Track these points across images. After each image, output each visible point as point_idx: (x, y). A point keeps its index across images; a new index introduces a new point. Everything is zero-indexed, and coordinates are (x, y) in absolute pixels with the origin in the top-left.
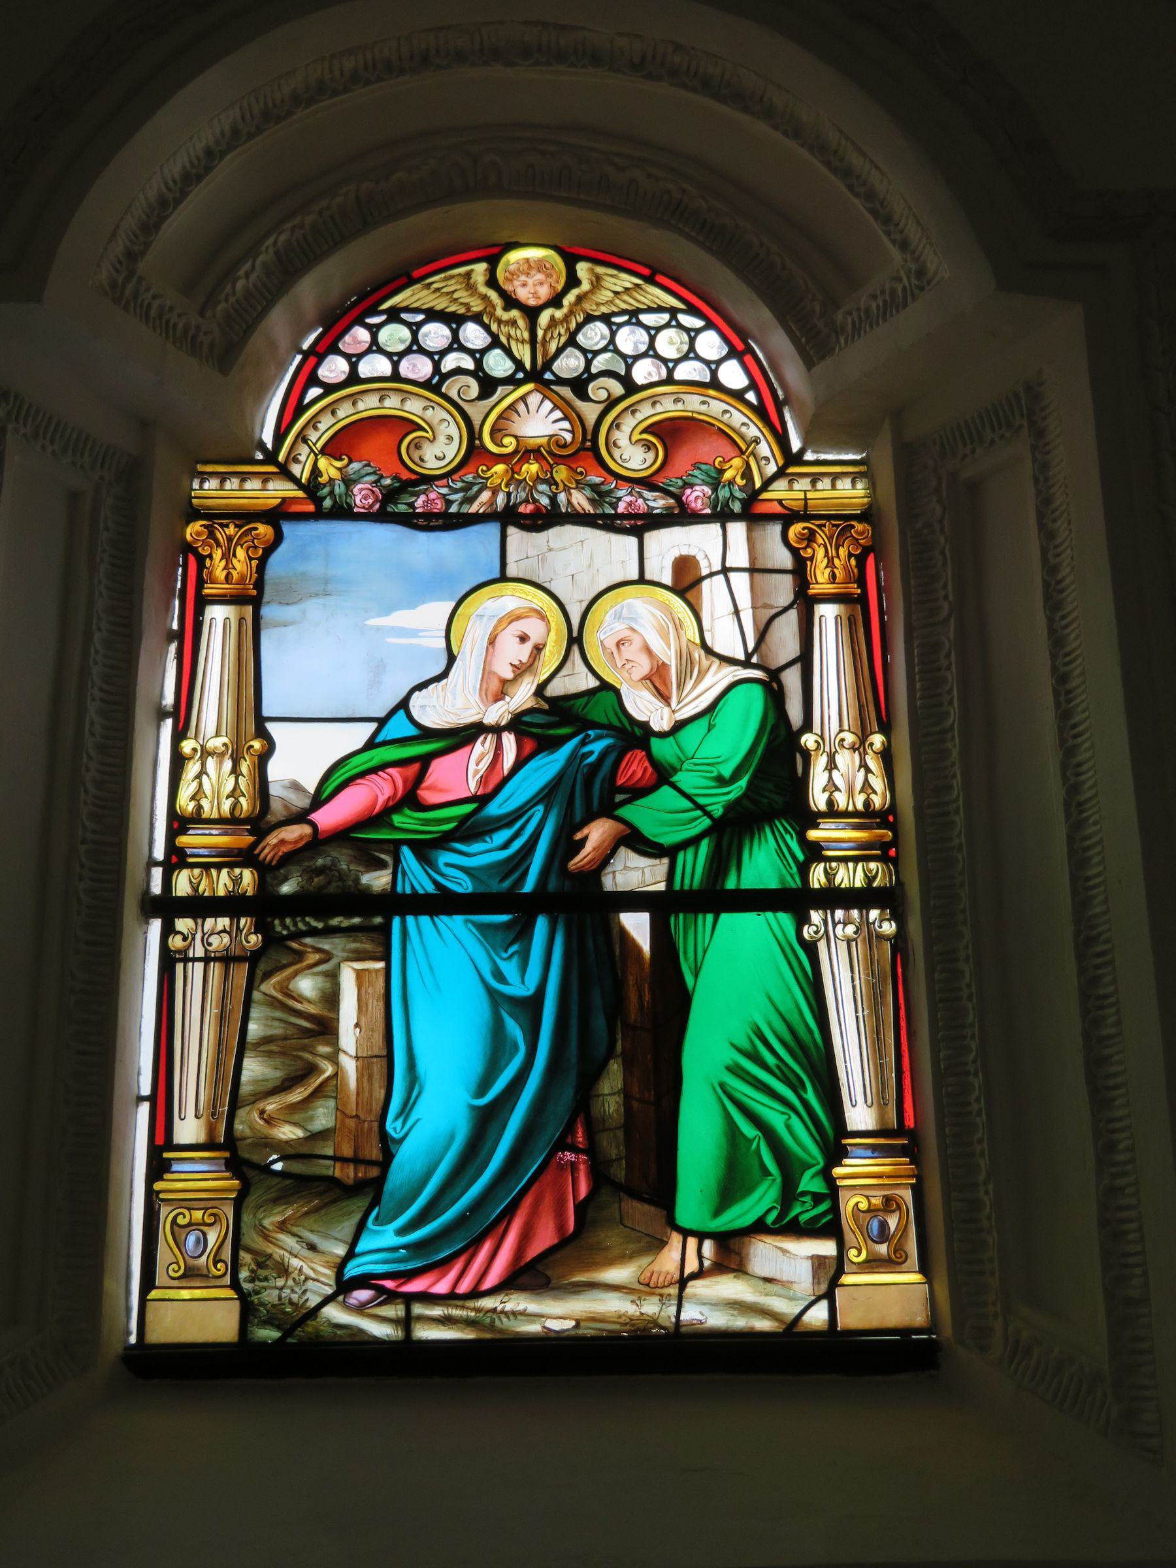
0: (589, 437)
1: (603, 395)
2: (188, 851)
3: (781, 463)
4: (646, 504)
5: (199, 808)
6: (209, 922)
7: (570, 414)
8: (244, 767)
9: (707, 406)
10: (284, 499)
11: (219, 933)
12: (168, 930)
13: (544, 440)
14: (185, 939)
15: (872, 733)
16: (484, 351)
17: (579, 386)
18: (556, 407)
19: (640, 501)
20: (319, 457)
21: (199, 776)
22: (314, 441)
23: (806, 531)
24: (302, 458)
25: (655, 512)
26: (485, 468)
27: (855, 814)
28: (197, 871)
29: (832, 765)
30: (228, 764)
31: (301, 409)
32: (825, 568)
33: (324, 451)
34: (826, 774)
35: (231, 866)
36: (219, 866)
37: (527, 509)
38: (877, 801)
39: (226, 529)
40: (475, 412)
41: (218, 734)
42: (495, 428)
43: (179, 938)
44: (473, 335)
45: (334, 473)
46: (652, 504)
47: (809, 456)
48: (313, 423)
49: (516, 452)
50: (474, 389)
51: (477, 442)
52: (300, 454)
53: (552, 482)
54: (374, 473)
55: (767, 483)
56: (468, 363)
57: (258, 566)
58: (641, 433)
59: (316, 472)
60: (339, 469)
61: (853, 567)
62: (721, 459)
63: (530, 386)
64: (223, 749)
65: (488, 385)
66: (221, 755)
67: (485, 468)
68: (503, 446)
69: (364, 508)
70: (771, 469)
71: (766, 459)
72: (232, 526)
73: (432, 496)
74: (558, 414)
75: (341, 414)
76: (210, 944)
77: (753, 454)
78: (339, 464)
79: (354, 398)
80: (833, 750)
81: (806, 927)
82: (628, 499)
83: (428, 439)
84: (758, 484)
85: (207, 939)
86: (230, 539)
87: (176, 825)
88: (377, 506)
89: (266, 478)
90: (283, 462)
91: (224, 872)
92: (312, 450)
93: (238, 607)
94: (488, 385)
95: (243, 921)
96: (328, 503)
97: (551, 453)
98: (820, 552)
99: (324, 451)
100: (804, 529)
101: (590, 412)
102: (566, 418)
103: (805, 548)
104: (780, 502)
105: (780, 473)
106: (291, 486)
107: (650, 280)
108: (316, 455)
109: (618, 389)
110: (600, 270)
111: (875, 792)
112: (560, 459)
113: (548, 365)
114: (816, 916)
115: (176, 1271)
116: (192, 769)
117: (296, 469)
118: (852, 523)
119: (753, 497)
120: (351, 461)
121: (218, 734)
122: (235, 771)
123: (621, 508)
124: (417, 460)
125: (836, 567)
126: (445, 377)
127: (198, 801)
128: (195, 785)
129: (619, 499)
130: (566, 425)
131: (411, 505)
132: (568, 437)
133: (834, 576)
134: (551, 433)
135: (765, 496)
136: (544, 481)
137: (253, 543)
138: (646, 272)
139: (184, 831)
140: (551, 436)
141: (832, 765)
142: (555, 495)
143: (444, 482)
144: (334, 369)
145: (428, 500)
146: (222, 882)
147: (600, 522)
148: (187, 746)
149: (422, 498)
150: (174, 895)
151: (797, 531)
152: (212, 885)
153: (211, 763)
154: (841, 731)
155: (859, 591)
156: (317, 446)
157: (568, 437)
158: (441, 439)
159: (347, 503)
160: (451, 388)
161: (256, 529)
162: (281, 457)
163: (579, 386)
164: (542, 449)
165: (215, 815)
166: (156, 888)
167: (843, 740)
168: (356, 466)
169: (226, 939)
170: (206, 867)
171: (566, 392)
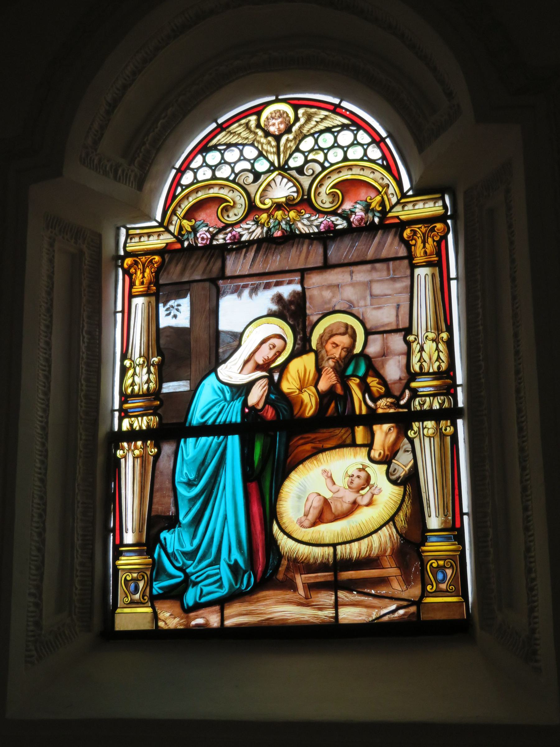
0: (306, 193)
1: (311, 172)
5: (133, 390)
7: (297, 184)
10: (167, 244)
13: (284, 200)
15: (442, 332)
22: (179, 213)
25: (338, 227)
30: (145, 370)
33: (185, 217)
37: (278, 234)
40: (252, 189)
48: (179, 205)
50: (251, 177)
55: (392, 207)
56: (249, 167)
59: (181, 228)
63: (276, 173)
65: (257, 176)
66: (142, 365)
68: (264, 204)
70: (394, 200)
77: (386, 193)
78: (190, 224)
80: (423, 342)
84: (388, 208)
87: (123, 399)
92: (178, 218)
98: (419, 241)
99: (185, 217)
101: (305, 182)
106: (170, 236)
108: (180, 220)
109: (318, 168)
113: (286, 162)
117: (172, 228)
121: (140, 357)
122: (149, 372)
125: (426, 248)
126: (236, 175)
132: (295, 195)
135: (390, 215)
139: (126, 402)
144: (187, 178)
147: (312, 236)
148: (127, 363)
155: (436, 259)
156: (181, 215)
157: (295, 195)
161: (154, 259)
162: (165, 224)
163: (300, 170)
167: (427, 336)
171: (294, 173)
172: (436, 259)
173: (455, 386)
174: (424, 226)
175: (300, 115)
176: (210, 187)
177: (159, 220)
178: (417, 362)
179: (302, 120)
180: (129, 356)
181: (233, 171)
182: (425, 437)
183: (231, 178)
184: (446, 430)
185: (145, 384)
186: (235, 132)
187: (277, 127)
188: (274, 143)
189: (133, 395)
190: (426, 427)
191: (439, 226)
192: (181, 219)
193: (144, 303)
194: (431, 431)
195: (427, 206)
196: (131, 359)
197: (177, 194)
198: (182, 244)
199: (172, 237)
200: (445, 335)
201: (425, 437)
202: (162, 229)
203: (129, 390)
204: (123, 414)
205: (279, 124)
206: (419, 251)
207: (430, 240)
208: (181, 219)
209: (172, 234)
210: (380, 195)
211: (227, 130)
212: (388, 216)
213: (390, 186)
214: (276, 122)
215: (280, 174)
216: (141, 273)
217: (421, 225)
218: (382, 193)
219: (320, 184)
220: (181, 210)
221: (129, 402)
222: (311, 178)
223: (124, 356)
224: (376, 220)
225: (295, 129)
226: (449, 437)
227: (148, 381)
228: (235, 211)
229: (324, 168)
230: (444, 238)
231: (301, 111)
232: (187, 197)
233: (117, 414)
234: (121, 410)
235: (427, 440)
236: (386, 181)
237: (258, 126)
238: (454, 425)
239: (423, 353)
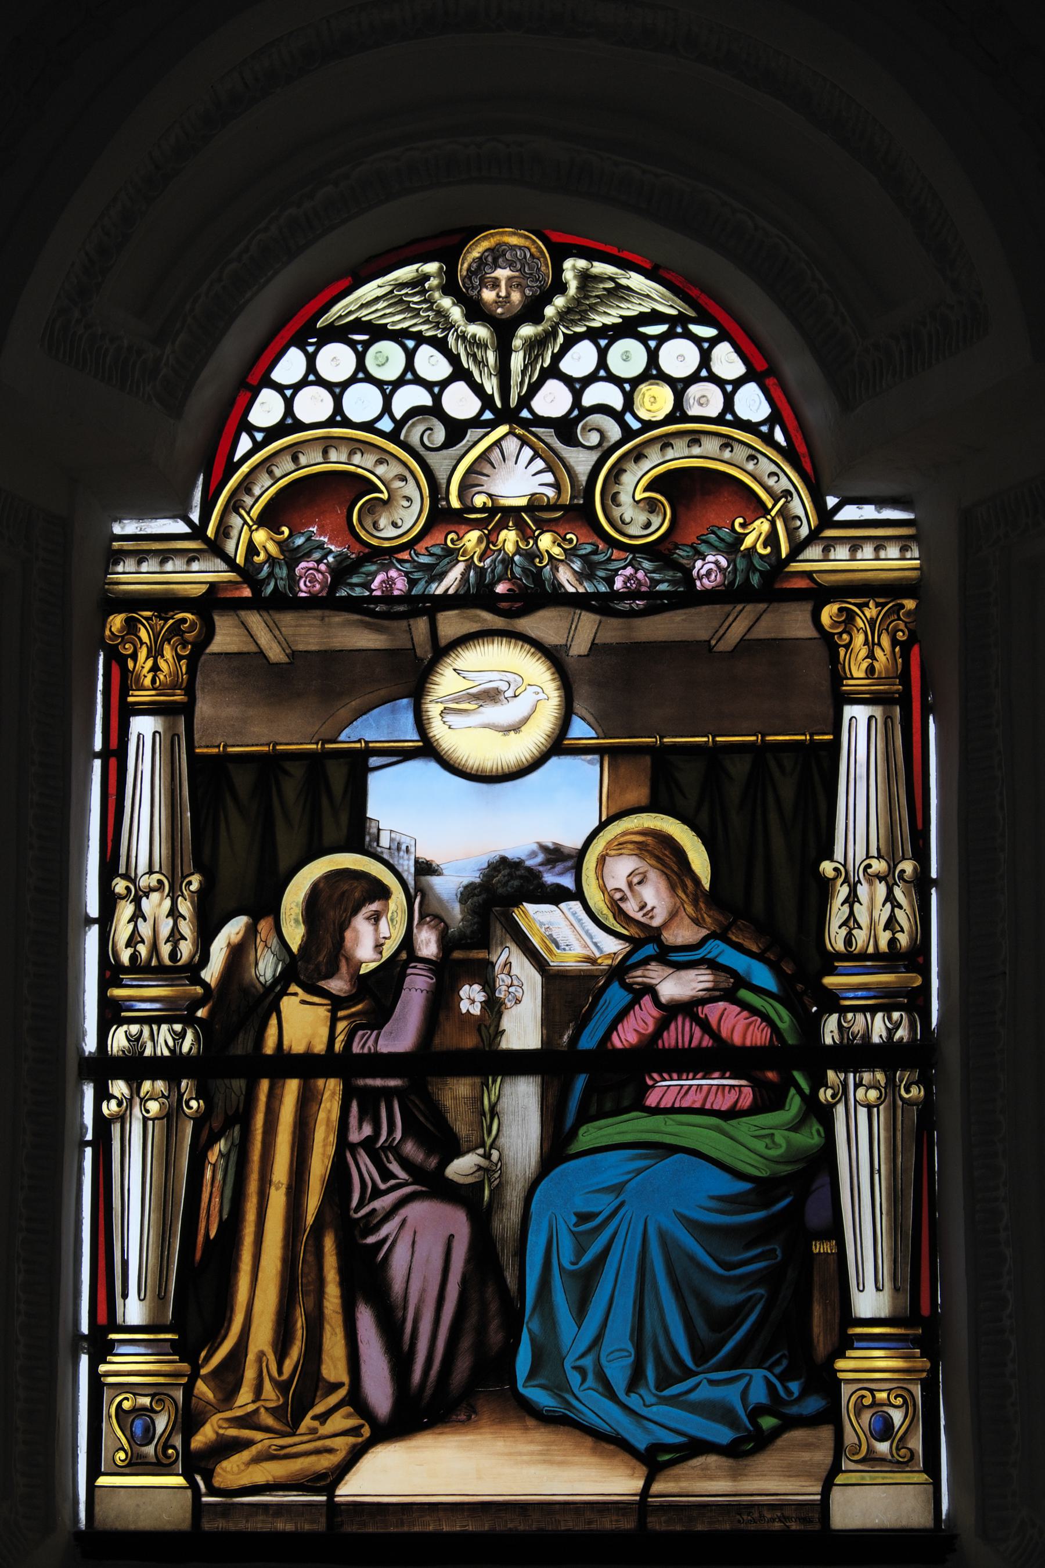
1: (594, 439)
7: (553, 463)
18: (537, 455)
21: (133, 919)
40: (439, 462)
41: (151, 872)
48: (246, 486)
55: (798, 548)
63: (503, 429)
74: (539, 464)
84: (784, 552)
89: (191, 556)
92: (245, 522)
104: (809, 575)
105: (814, 536)
106: (221, 565)
108: (250, 527)
109: (615, 432)
116: (125, 910)
121: (151, 872)
128: (131, 926)
130: (549, 478)
134: (531, 493)
135: (795, 567)
162: (210, 532)
171: (548, 434)
176: (327, 444)
180: (122, 870)
183: (386, 425)
192: (251, 523)
197: (236, 459)
203: (125, 957)
207: (886, 641)
208: (251, 523)
213: (795, 495)
215: (511, 433)
218: (773, 513)
219: (616, 473)
223: (109, 869)
236: (785, 484)
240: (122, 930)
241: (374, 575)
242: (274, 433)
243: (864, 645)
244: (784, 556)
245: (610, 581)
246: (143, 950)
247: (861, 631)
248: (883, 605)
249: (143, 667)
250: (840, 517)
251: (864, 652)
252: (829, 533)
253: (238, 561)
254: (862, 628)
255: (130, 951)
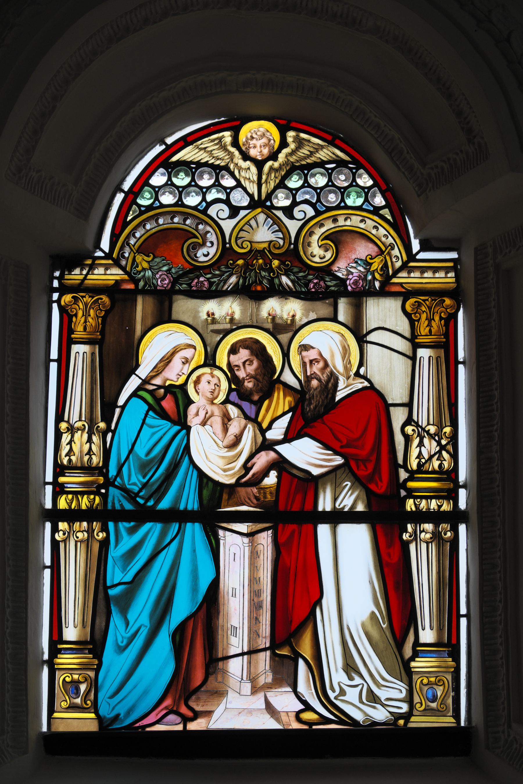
0: (293, 241)
2: (65, 485)
3: (405, 258)
4: (326, 284)
5: (70, 461)
6: (77, 525)
8: (95, 438)
9: (364, 222)
10: (117, 281)
11: (82, 532)
12: (55, 530)
13: (266, 245)
14: (64, 534)
15: (446, 426)
16: (232, 189)
17: (288, 211)
18: (274, 223)
19: (322, 283)
20: (136, 255)
21: (70, 443)
22: (133, 244)
23: (417, 303)
24: (126, 255)
26: (231, 262)
27: (434, 472)
28: (70, 496)
29: (421, 444)
30: (85, 436)
31: (126, 224)
32: (426, 327)
33: (140, 251)
34: (418, 449)
35: (88, 493)
36: (82, 493)
38: (446, 464)
39: (84, 299)
40: (228, 226)
41: (80, 420)
42: (239, 236)
43: (61, 533)
44: (228, 182)
45: (145, 265)
46: (329, 284)
47: (422, 256)
48: (132, 233)
49: (251, 251)
50: (226, 211)
51: (228, 246)
52: (125, 252)
53: (271, 270)
54: (169, 264)
55: (396, 272)
56: (223, 196)
57: (102, 321)
58: (322, 241)
60: (148, 262)
61: (443, 325)
62: (370, 257)
63: (259, 210)
64: (83, 427)
65: (234, 211)
66: (83, 430)
67: (231, 262)
68: (243, 248)
69: (162, 286)
70: (398, 264)
71: (397, 257)
72: (87, 297)
73: (202, 279)
74: (276, 227)
75: (148, 227)
76: (78, 538)
77: (389, 254)
79: (156, 218)
81: (404, 534)
82: (315, 281)
83: (199, 243)
84: (391, 272)
85: (76, 534)
86: (86, 304)
87: (58, 470)
88: (169, 286)
89: (107, 267)
90: (116, 258)
91: (85, 496)
93: (92, 346)
94: (234, 211)
95: (95, 523)
96: (141, 284)
97: (270, 251)
99: (140, 251)
100: (415, 302)
101: (293, 226)
102: (280, 230)
103: (415, 313)
104: (401, 284)
105: (404, 266)
106: (121, 272)
107: (332, 143)
108: (135, 253)
109: (311, 212)
110: (303, 135)
111: (445, 460)
112: (276, 256)
113: (269, 196)
114: (409, 527)
115: (64, 704)
116: (66, 438)
117: (123, 263)
118: (443, 298)
119: (386, 280)
120: (155, 257)
121: (80, 420)
122: (90, 440)
123: (312, 285)
124: (192, 255)
125: (433, 327)
126: (209, 204)
127: (70, 457)
128: (69, 446)
129: (310, 281)
131: (189, 285)
132: (281, 242)
133: (430, 331)
135: (395, 280)
136: (264, 270)
137: (99, 307)
138: (330, 138)
140: (271, 242)
141: (421, 444)
142: (273, 279)
143: (207, 271)
144: (145, 201)
145: (199, 282)
146: (85, 502)
148: (63, 426)
149: (196, 281)
150: (58, 508)
151: (411, 303)
152: (79, 504)
153: (77, 435)
154: (428, 424)
155: (444, 340)
156: (135, 247)
157: (281, 242)
158: (209, 244)
159: (153, 283)
160: (212, 211)
161: (101, 299)
162: (115, 255)
163: (288, 211)
164: (266, 251)
165: (79, 465)
166: (48, 505)
168: (157, 260)
169: (86, 534)
170: (75, 493)
171: (280, 214)
172: (444, 340)
173: (457, 486)
174: (432, 298)
175: (290, 140)
176: (174, 215)
177: (107, 250)
178: (416, 459)
179: (293, 146)
180: (66, 418)
181: (204, 199)
182: (422, 543)
184: (445, 534)
185: (86, 455)
186: (205, 148)
187: (259, 150)
188: (254, 169)
189: (71, 468)
190: (423, 531)
191: (448, 302)
192: (135, 252)
193: (86, 353)
194: (428, 536)
195: (437, 275)
196: (68, 422)
198: (137, 285)
199: (122, 273)
200: (447, 430)
201: (422, 543)
202: (110, 262)
203: (65, 461)
204: (58, 489)
205: (261, 147)
206: (423, 329)
207: (437, 318)
208: (135, 252)
209: (123, 269)
210: (383, 255)
211: (194, 144)
212: (392, 281)
214: (259, 143)
215: (262, 212)
216: (83, 315)
217: (428, 297)
218: (385, 254)
219: (311, 233)
220: (135, 240)
221: (66, 474)
222: (301, 222)
223: (59, 418)
224: (377, 284)
225: (282, 157)
226: (449, 543)
227: (90, 452)
228: (204, 250)
229: (318, 213)
230: (454, 316)
231: (291, 135)
232: (142, 224)
233: (49, 489)
234: (55, 483)
235: (424, 546)
236: (390, 240)
237: (235, 143)
238: (455, 530)
239: (423, 448)
240: (65, 449)
241: (193, 280)
242: (150, 208)
243: (426, 320)
244: (390, 274)
245: (307, 285)
246: (73, 458)
247: (425, 312)
248: (435, 300)
249: (80, 321)
250: (418, 257)
251: (427, 322)
252: (412, 264)
253: (127, 270)
254: (425, 311)
255: (68, 458)
